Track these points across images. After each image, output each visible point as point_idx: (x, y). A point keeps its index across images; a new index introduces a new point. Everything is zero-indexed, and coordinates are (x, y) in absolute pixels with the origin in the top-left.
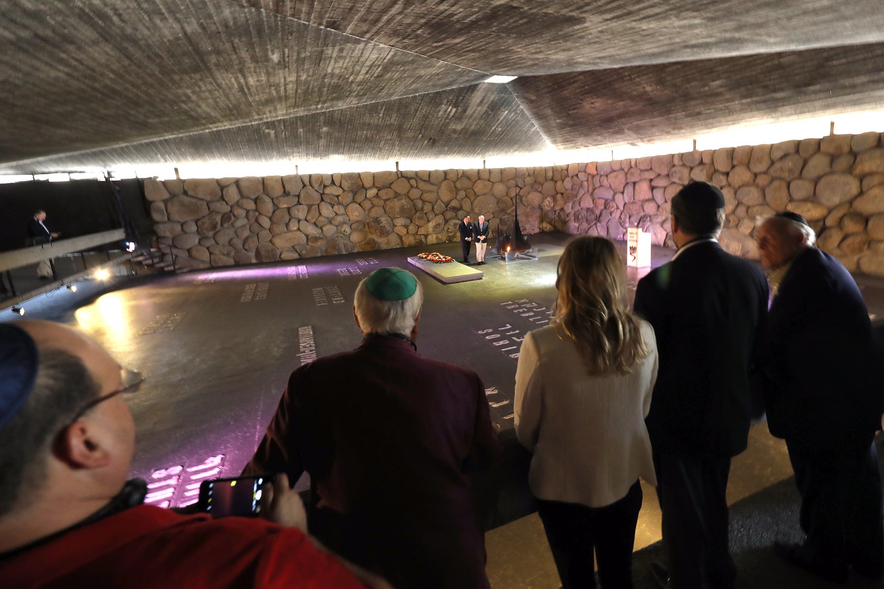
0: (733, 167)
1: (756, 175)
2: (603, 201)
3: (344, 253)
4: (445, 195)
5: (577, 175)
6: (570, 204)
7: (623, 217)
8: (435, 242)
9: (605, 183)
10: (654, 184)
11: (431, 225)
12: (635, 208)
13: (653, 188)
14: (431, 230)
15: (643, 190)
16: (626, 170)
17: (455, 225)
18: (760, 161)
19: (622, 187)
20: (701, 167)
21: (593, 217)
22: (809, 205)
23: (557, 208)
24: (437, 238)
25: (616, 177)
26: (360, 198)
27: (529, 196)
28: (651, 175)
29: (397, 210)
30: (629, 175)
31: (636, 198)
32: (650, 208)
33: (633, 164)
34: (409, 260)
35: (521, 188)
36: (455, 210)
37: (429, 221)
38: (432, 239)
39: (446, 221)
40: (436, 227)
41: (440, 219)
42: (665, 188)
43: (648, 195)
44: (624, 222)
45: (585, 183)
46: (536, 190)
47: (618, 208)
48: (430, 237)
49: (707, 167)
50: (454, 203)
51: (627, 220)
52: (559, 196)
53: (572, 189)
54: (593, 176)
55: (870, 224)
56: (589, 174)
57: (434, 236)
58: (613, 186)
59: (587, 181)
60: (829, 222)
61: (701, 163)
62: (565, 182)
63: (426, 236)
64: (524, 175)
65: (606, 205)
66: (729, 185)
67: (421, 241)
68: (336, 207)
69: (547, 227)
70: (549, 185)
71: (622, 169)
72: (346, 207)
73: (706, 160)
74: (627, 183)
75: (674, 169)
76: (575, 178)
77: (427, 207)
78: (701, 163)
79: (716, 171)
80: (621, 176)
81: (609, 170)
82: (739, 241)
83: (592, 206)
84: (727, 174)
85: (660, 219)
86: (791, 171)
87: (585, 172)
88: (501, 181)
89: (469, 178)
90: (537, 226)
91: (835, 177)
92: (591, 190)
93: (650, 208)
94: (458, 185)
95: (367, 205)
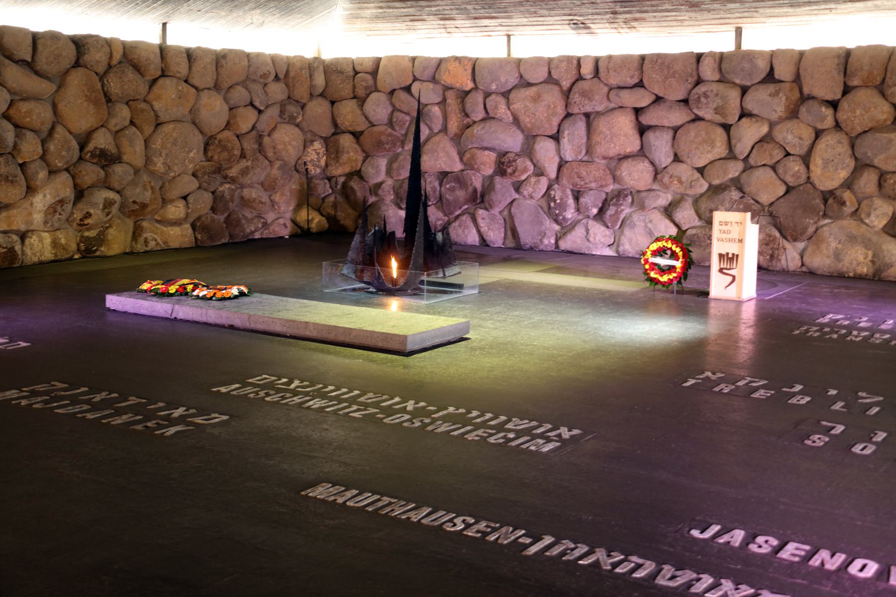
0: (847, 90)
2: (493, 156)
4: (80, 114)
5: (408, 89)
6: (383, 163)
7: (557, 193)
8: (48, 255)
9: (502, 110)
10: (646, 120)
11: (41, 201)
12: (594, 175)
13: (642, 130)
14: (38, 218)
15: (620, 133)
16: (566, 84)
17: (108, 204)
19: (555, 122)
20: (771, 88)
21: (461, 194)
23: (339, 171)
24: (55, 244)
25: (536, 99)
27: (276, 135)
28: (643, 99)
30: (575, 97)
31: (600, 150)
32: (637, 175)
33: (587, 70)
34: (113, 301)
35: (260, 112)
36: (107, 159)
37: (31, 190)
38: (40, 248)
39: (80, 194)
40: (52, 210)
41: (63, 186)
42: (676, 130)
43: (633, 144)
44: (563, 206)
45: (436, 110)
46: (292, 120)
47: (540, 172)
48: (33, 240)
49: (787, 86)
50: (102, 140)
51: (571, 201)
52: (346, 141)
53: (391, 123)
56: (447, 88)
57: (47, 238)
58: (525, 120)
59: (443, 103)
61: (770, 77)
62: (369, 106)
63: (23, 236)
65: (503, 166)
66: (838, 126)
67: (12, 250)
69: (317, 221)
70: (318, 109)
71: (550, 80)
73: (784, 72)
74: (568, 115)
75: (701, 89)
76: (403, 95)
77: (30, 147)
78: (770, 77)
79: (805, 98)
80: (552, 98)
81: (512, 80)
82: (867, 244)
83: (458, 167)
84: (834, 105)
85: (664, 199)
87: (434, 80)
88: (217, 87)
89: (137, 68)
90: (289, 215)
92: (454, 125)
93: (637, 175)
94: (114, 86)
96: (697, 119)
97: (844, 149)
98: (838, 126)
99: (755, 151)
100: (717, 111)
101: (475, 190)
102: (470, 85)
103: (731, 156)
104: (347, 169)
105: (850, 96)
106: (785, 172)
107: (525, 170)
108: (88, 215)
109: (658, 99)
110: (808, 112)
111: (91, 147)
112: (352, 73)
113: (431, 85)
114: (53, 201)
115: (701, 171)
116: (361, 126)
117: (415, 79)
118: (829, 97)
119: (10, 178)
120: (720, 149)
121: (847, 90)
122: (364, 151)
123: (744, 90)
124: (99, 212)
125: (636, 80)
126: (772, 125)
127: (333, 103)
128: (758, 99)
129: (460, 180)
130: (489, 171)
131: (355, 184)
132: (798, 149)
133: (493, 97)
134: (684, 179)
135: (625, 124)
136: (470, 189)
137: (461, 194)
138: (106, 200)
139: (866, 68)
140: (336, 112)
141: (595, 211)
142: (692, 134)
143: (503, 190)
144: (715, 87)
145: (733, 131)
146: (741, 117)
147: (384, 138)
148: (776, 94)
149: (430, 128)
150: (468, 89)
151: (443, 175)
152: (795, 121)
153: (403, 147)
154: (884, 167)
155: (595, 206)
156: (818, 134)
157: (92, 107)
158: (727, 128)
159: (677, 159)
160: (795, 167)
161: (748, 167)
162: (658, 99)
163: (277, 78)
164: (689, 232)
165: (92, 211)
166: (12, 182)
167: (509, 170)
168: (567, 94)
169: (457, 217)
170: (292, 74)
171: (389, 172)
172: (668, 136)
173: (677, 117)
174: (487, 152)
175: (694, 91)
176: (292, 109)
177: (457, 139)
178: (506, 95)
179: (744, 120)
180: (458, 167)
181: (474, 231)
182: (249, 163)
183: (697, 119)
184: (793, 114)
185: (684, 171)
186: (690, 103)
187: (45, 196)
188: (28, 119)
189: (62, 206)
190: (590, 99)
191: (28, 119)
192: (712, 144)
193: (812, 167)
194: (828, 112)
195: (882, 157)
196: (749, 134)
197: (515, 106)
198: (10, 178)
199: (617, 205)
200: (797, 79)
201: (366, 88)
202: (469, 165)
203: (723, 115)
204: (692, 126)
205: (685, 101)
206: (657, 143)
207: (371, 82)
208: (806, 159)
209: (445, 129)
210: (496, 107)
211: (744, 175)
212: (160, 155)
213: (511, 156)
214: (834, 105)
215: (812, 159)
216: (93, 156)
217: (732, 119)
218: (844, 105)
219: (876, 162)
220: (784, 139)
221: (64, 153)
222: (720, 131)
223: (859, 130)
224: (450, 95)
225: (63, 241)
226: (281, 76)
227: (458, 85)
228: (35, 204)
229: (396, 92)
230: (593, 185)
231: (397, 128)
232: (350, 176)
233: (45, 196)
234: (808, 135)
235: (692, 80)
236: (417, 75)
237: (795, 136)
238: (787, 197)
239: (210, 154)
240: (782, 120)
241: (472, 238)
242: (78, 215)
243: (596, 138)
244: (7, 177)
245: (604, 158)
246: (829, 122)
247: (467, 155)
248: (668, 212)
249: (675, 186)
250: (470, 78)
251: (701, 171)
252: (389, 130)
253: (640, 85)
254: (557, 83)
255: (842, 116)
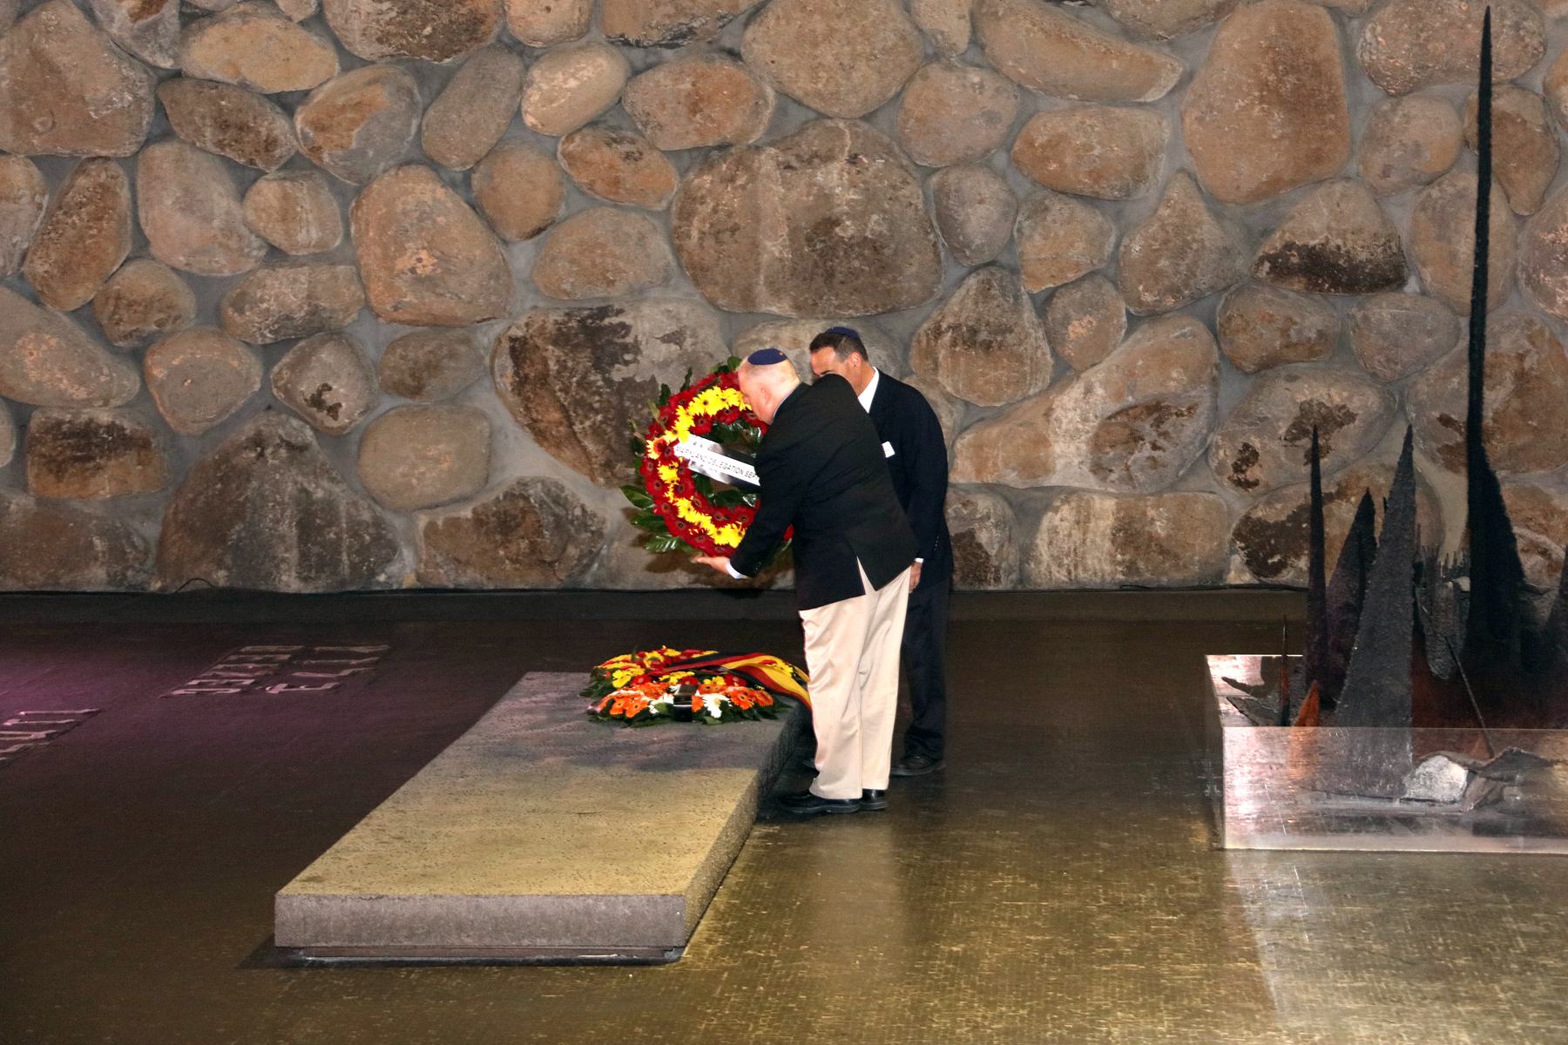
3: (290, 582)
14: (1067, 456)
24: (1129, 534)
26: (463, 124)
29: (775, 247)
37: (1064, 373)
48: (1060, 519)
57: (1105, 509)
68: (268, 191)
72: (351, 190)
95: (525, 182)
114: (1114, 407)
119: (983, 336)
124: (1276, 446)
138: (1305, 410)
157: (1278, 116)
165: (1256, 443)
166: (987, 346)
187: (1088, 390)
188: (1053, 167)
189: (1158, 422)
191: (1053, 167)
198: (983, 336)
221: (1163, 263)
225: (1160, 528)
228: (1058, 413)
233: (1088, 390)
244: (974, 332)
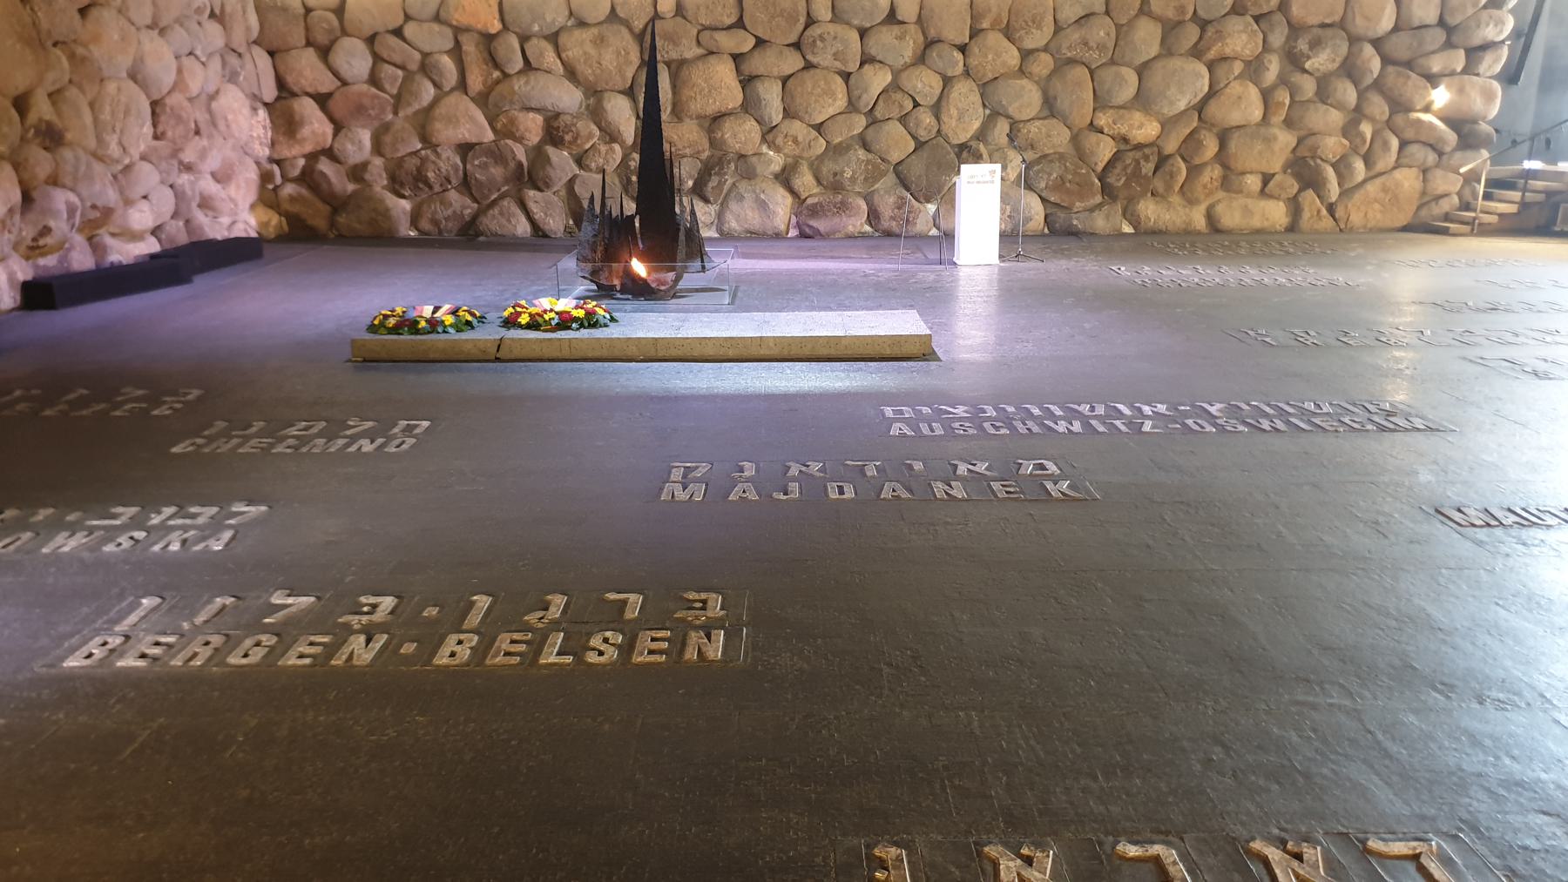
1: (1026, 54)
2: (539, 119)
5: (398, 32)
6: (366, 137)
13: (747, 81)
16: (638, 25)
18: (1037, 22)
20: (896, 30)
22: (1138, 116)
25: (600, 41)
42: (785, 81)
45: (447, 63)
52: (307, 108)
53: (374, 80)
54: (488, 39)
55: (1233, 145)
56: (458, 31)
58: (586, 71)
60: (1171, 146)
64: (199, 11)
65: (554, 133)
75: (815, 31)
76: (393, 41)
85: (776, 161)
86: (1101, 47)
91: (1176, 63)
96: (809, 66)
97: (976, 98)
98: (967, 73)
99: (881, 102)
100: (836, 56)
101: (520, 165)
102: (496, 26)
103: (852, 106)
104: (308, 148)
105: (980, 39)
106: (917, 125)
107: (591, 135)
108: (46, 231)
109: (760, 43)
110: (940, 56)
111: (32, 118)
112: (302, 11)
113: (436, 27)
115: (819, 128)
116: (327, 83)
117: (408, 18)
118: (958, 42)
120: (841, 102)
121: (975, 33)
122: (332, 119)
123: (863, 33)
125: (733, 19)
126: (896, 74)
127: (271, 54)
128: (883, 42)
129: (496, 154)
130: (534, 138)
131: (325, 166)
132: (927, 100)
133: (534, 41)
134: (800, 139)
135: (724, 72)
136: (512, 165)
137: (497, 172)
139: (994, 10)
140: (282, 69)
141: (690, 183)
142: (809, 85)
143: (561, 161)
144: (832, 28)
145: (852, 80)
146: (862, 64)
147: (366, 102)
148: (901, 38)
149: (436, 85)
150: (493, 31)
151: (465, 149)
152: (922, 67)
153: (396, 113)
154: (1017, 117)
155: (691, 177)
156: (947, 81)
158: (847, 76)
159: (788, 114)
160: (927, 119)
161: (873, 122)
162: (760, 43)
163: (212, 15)
164: (809, 201)
167: (568, 138)
168: (640, 37)
169: (494, 203)
170: (228, 9)
171: (377, 148)
172: (777, 87)
173: (792, 62)
174: (531, 115)
175: (809, 32)
176: (233, 60)
177: (482, 100)
178: (554, 38)
179: (866, 66)
180: (489, 136)
181: (523, 219)
182: (205, 142)
183: (809, 66)
184: (921, 59)
185: (797, 128)
186: (804, 48)
190: (676, 44)
192: (833, 95)
193: (944, 118)
194: (958, 56)
195: (1017, 104)
196: (878, 80)
197: (570, 53)
199: (721, 174)
200: (920, 20)
201: (330, 31)
202: (507, 132)
203: (844, 62)
204: (807, 75)
205: (797, 46)
206: (768, 97)
207: (336, 23)
208: (937, 109)
209: (462, 85)
210: (541, 55)
211: (871, 130)
212: (114, 131)
213: (568, 119)
214: (963, 49)
215: (944, 110)
216: (38, 132)
217: (853, 66)
218: (975, 49)
219: (1011, 111)
220: (915, 87)
222: (839, 80)
223: (990, 76)
224: (463, 38)
226: (217, 11)
227: (479, 26)
229: (378, 38)
230: (688, 151)
231: (387, 87)
232: (312, 157)
234: (937, 83)
235: (802, 20)
236: (410, 12)
237: (925, 83)
238: (919, 153)
239: (160, 129)
240: (907, 67)
241: (522, 228)
242: (29, 233)
243: (686, 93)
245: (699, 117)
246: (960, 68)
247: (503, 119)
248: (785, 178)
249: (790, 148)
250: (497, 16)
251: (819, 128)
252: (374, 90)
253: (740, 24)
254: (626, 23)
255: (973, 62)
